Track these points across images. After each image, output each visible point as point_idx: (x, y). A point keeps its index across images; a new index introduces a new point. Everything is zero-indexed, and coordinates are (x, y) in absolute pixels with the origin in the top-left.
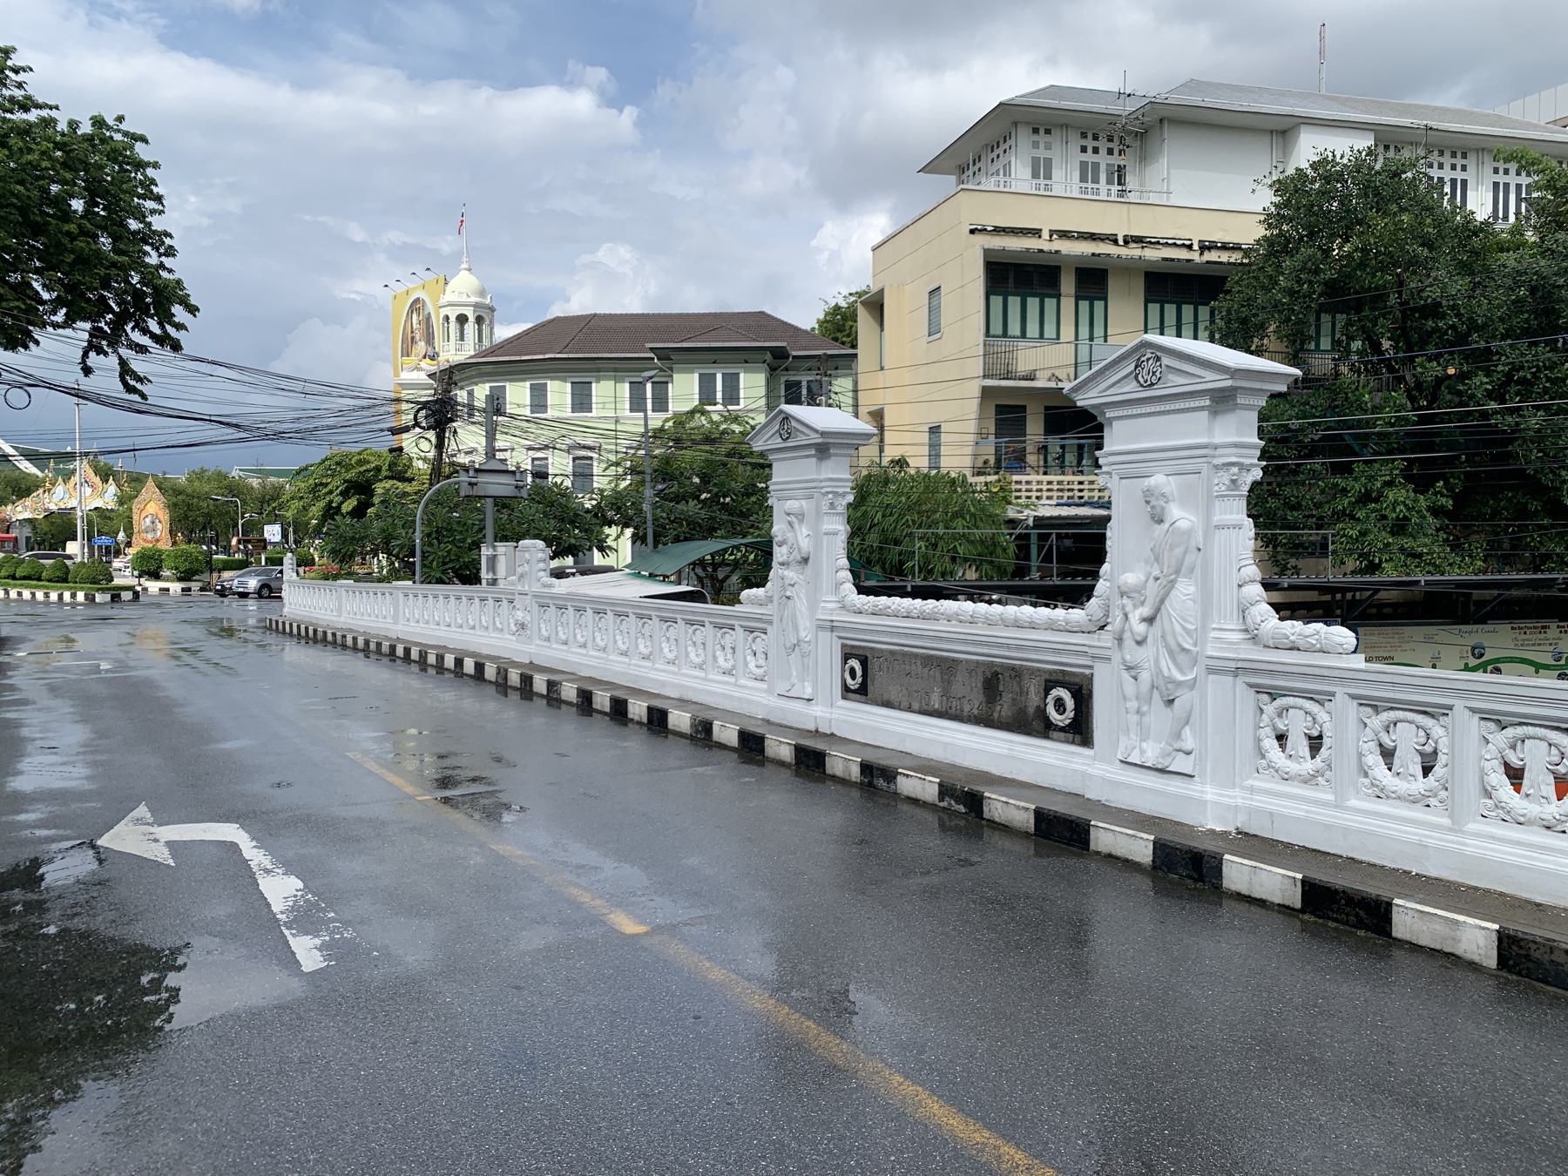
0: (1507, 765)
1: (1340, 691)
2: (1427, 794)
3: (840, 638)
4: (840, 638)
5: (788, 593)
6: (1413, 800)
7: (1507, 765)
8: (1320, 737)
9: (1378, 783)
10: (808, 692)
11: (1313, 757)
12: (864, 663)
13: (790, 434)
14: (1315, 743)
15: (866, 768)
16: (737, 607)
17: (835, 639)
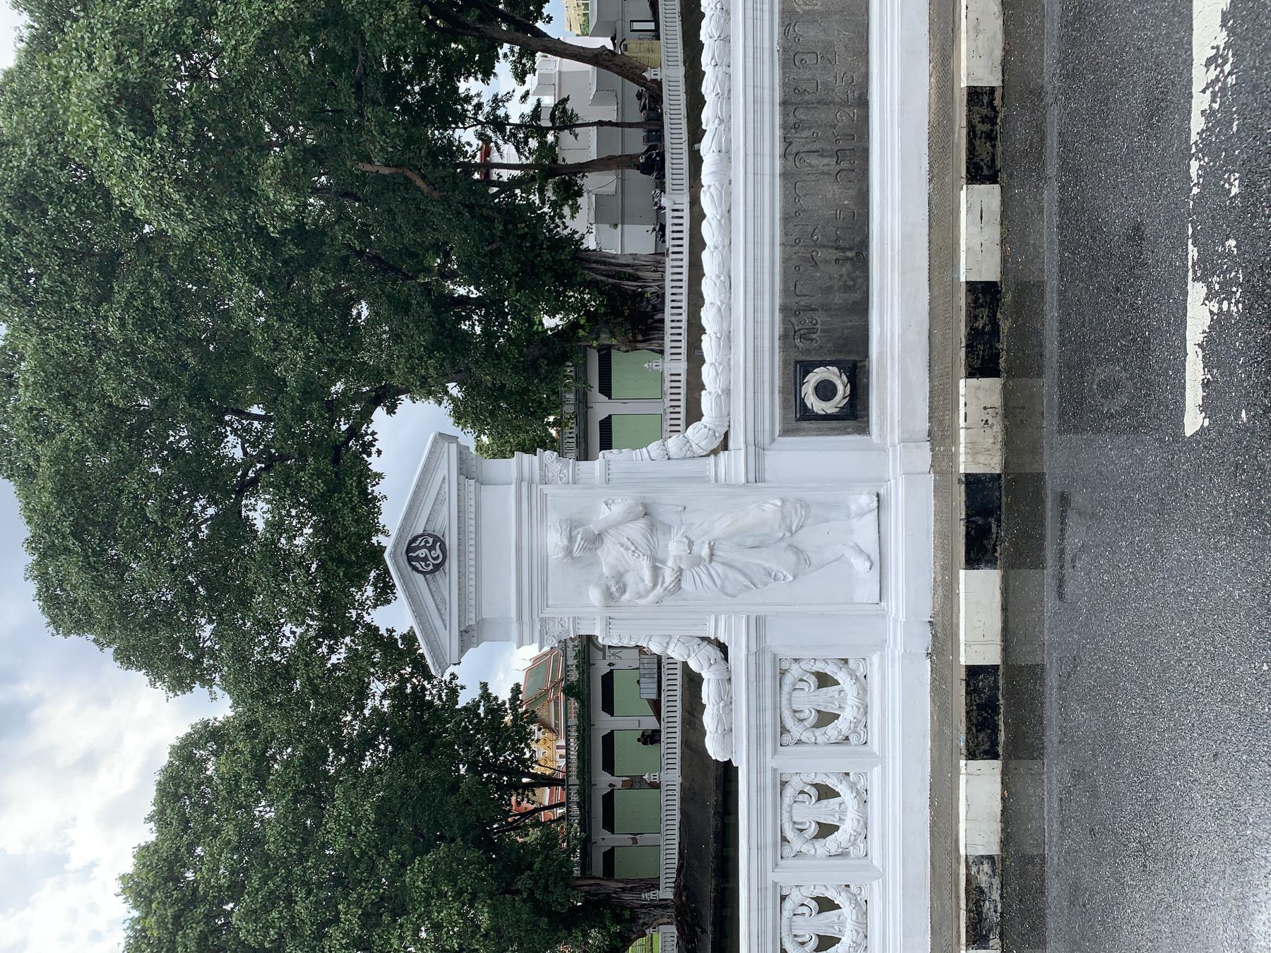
0: (816, 837)
1: (771, 877)
2: (853, 901)
3: (773, 440)
4: (773, 440)
5: (705, 552)
6: (863, 691)
7: (816, 837)
8: (817, 899)
9: (852, 838)
10: (866, 500)
11: (838, 907)
12: (806, 368)
13: (436, 539)
14: (826, 793)
15: (978, 553)
16: (741, 763)
17: (774, 445)
